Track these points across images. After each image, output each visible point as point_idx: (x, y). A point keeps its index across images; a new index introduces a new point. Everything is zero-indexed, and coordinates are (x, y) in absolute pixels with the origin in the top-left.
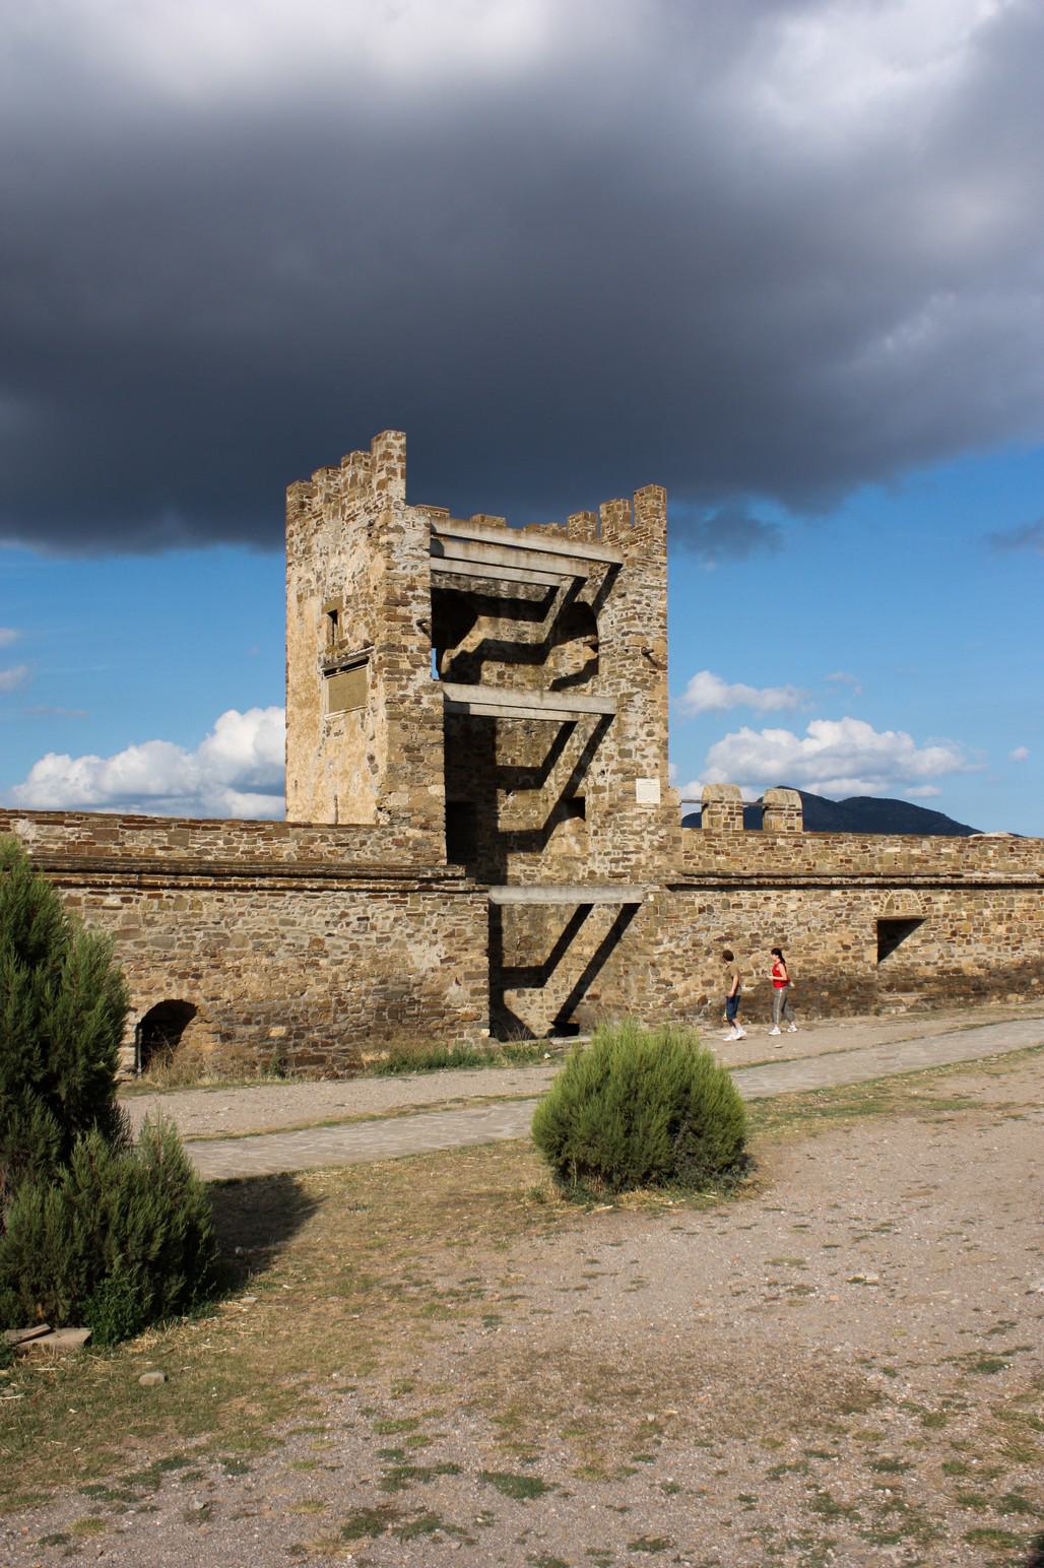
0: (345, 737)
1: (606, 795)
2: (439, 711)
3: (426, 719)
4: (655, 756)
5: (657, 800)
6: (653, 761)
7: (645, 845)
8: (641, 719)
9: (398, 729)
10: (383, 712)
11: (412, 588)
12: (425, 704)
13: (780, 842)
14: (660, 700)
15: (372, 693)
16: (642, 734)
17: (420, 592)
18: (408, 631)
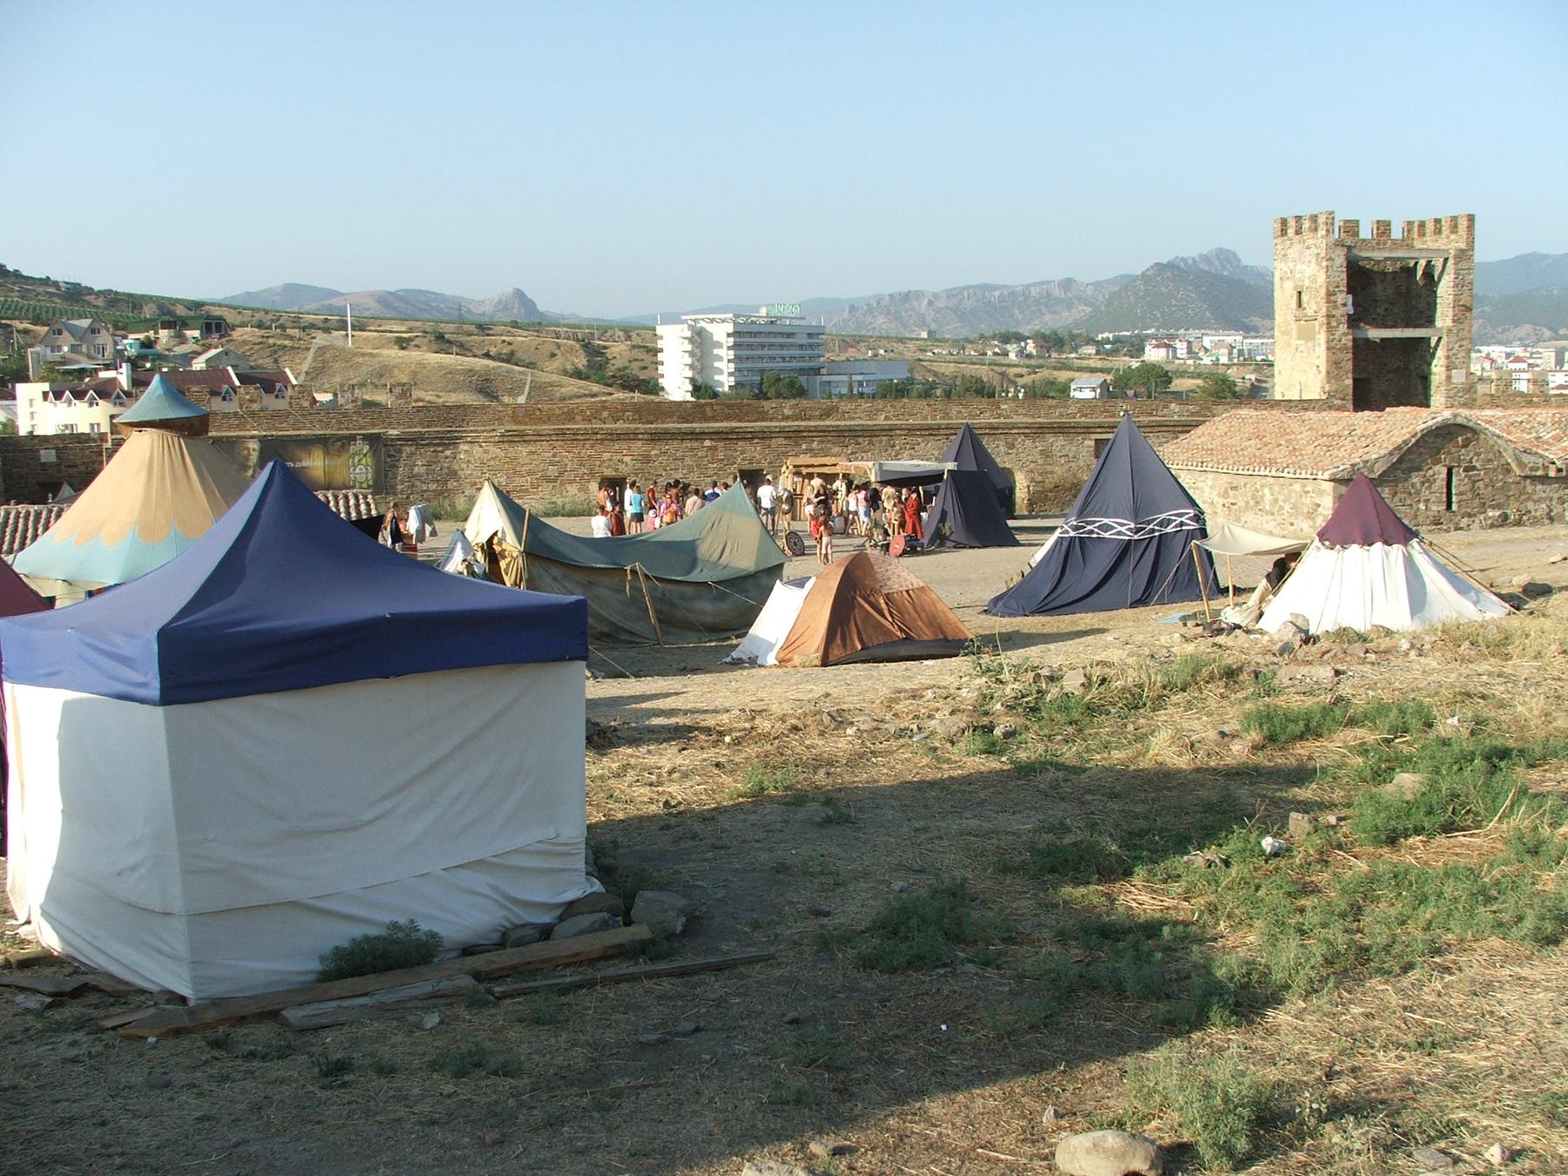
0: (1305, 354)
1: (1437, 377)
2: (1350, 344)
3: (1345, 348)
4: (1464, 357)
5: (1463, 380)
6: (1461, 360)
7: (1456, 403)
8: (1457, 339)
9: (1331, 354)
10: (1323, 346)
11: (1338, 287)
12: (1344, 341)
13: (1535, 399)
14: (1467, 328)
15: (1318, 336)
16: (1457, 346)
17: (1342, 288)
18: (1336, 307)
